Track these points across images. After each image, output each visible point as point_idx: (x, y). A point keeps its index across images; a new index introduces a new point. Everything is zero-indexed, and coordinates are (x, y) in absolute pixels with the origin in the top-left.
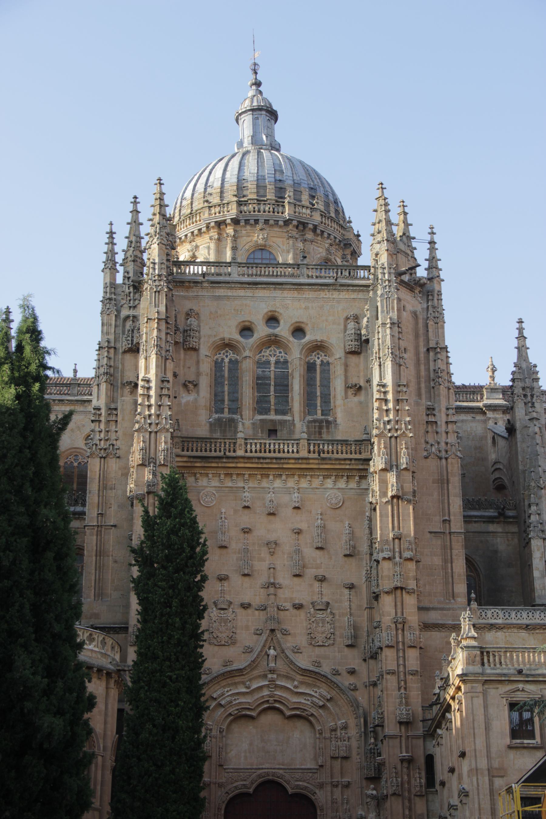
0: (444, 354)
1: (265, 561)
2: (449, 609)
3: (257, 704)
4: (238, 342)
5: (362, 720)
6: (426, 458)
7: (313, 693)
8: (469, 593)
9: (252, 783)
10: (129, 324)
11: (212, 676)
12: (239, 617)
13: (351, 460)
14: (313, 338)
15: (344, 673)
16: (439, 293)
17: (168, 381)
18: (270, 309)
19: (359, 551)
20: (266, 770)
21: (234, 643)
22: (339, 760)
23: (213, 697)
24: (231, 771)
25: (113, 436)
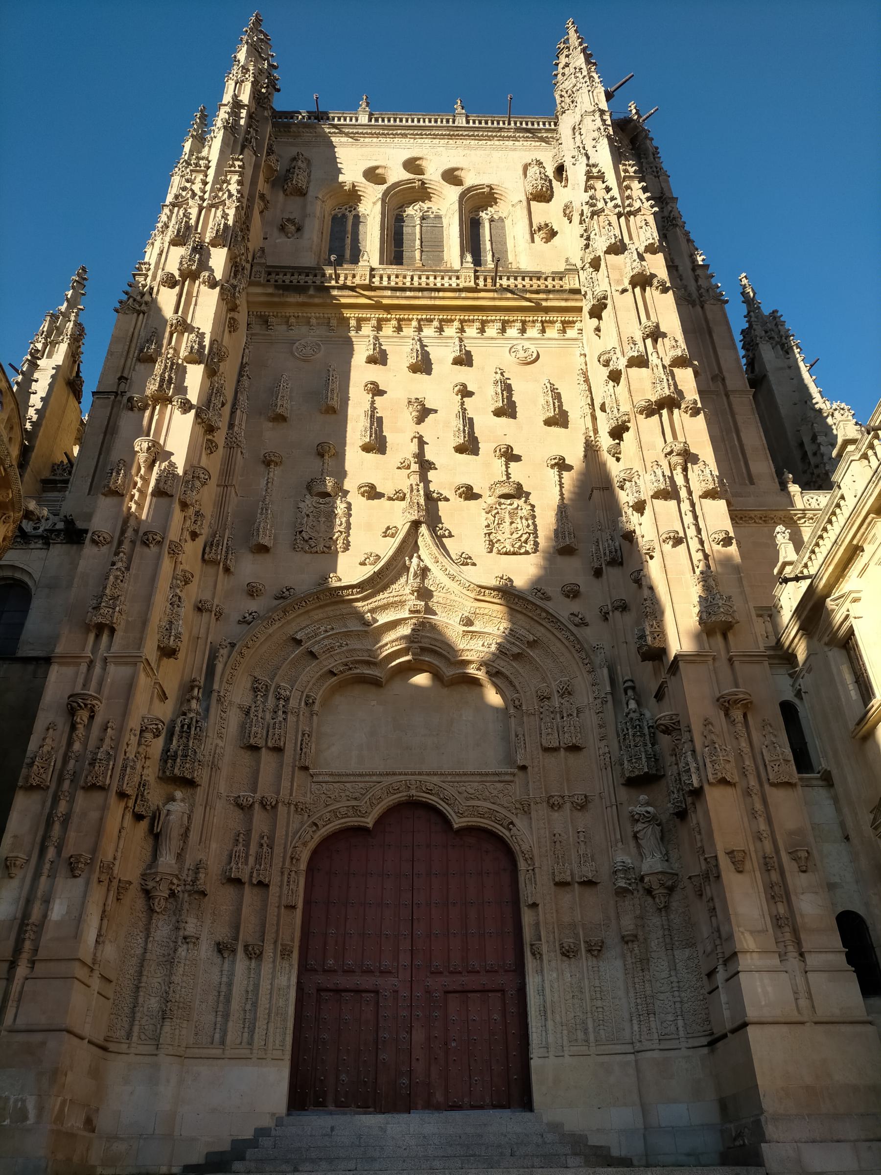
9: (372, 805)
24: (327, 779)
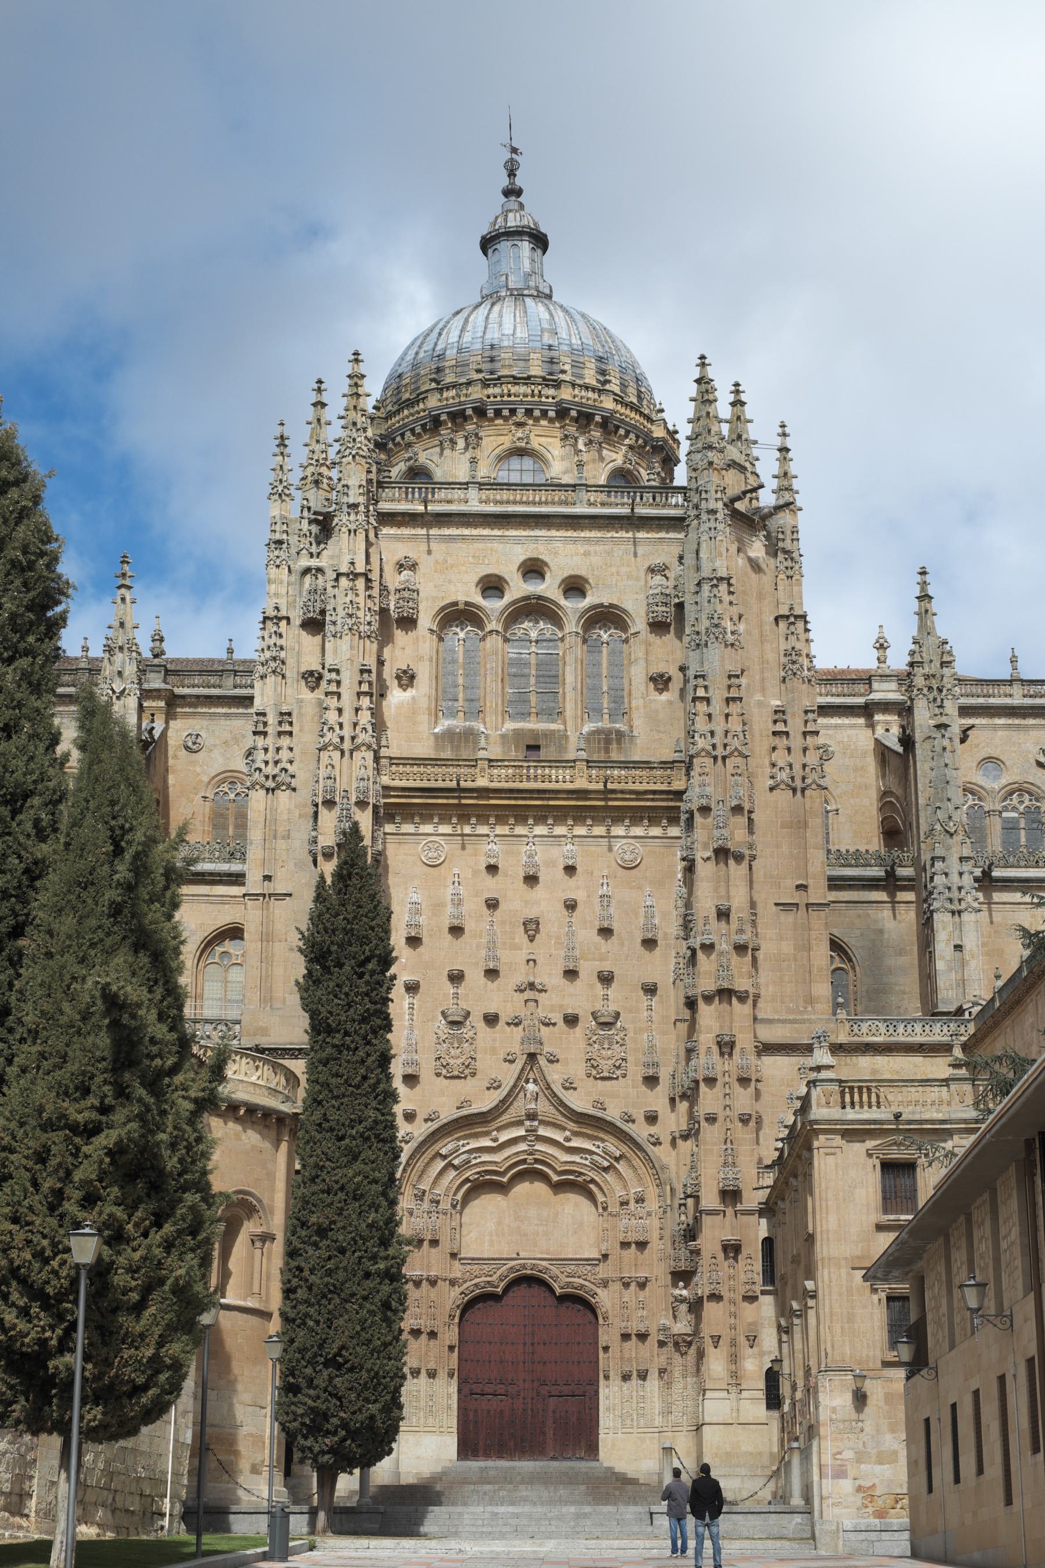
0: (800, 625)
1: (521, 949)
2: (803, 1021)
3: (508, 1164)
4: (478, 607)
5: (668, 1188)
6: (772, 789)
7: (594, 1149)
8: (835, 998)
10: (308, 579)
11: (440, 1123)
12: (480, 1035)
13: (654, 792)
14: (597, 601)
15: (641, 1119)
16: (795, 531)
17: (369, 671)
18: (529, 555)
19: (666, 934)
20: (522, 1262)
21: (473, 1074)
22: (633, 1246)
23: (441, 1155)
25: (284, 755)
